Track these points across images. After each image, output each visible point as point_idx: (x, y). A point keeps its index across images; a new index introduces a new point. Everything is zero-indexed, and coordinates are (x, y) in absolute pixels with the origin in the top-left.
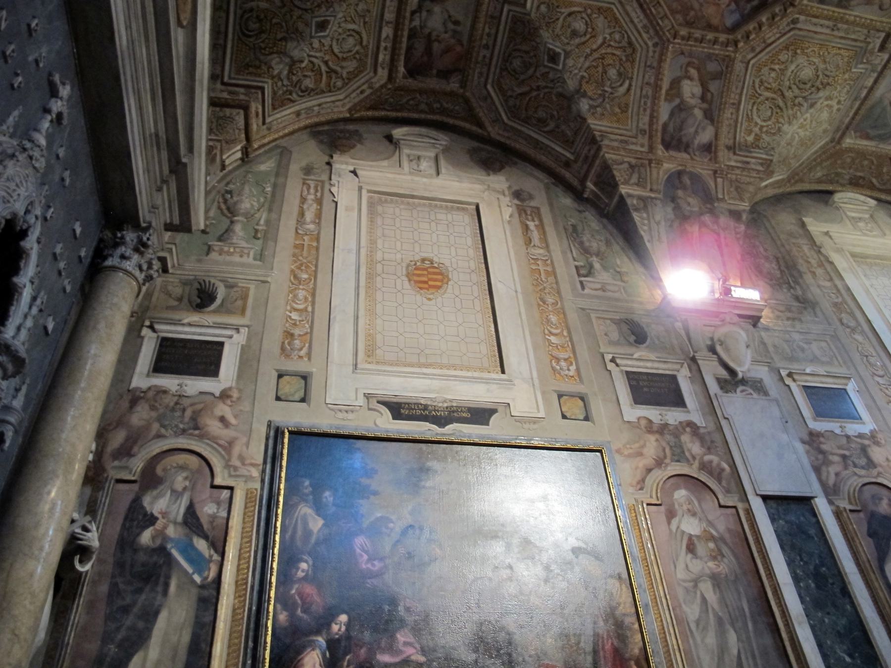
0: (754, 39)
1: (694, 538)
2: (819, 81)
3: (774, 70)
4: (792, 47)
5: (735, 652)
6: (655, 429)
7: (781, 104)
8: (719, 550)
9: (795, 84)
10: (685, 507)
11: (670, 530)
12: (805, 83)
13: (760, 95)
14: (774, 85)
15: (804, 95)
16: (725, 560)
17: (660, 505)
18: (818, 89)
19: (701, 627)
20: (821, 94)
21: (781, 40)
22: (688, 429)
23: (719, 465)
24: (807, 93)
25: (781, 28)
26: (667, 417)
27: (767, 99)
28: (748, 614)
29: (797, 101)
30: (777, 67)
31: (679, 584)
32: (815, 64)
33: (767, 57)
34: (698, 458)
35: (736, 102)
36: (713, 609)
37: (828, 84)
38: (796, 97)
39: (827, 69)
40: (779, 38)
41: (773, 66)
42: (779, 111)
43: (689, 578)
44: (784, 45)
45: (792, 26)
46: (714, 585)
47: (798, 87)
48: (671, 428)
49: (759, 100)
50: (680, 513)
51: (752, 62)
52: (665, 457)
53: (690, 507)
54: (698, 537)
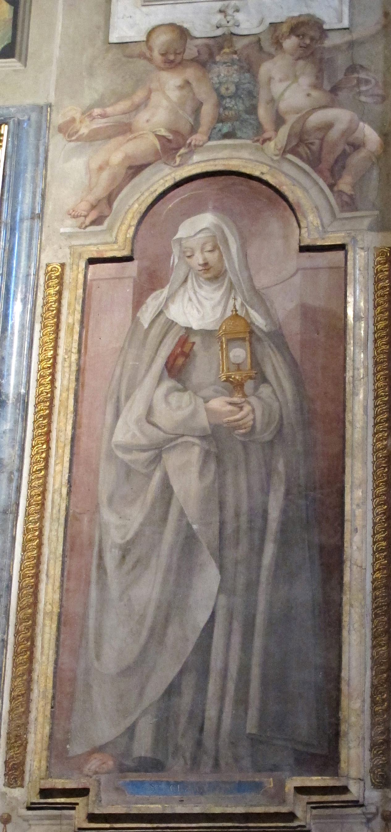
1: (196, 339)
5: (202, 618)
6: (191, 51)
8: (256, 363)
10: (198, 259)
11: (135, 320)
16: (265, 390)
17: (128, 259)
19: (130, 560)
22: (290, 43)
23: (350, 130)
26: (240, 16)
28: (273, 525)
31: (111, 456)
34: (291, 119)
36: (182, 513)
43: (144, 441)
46: (207, 454)
48: (239, 44)
50: (177, 275)
52: (194, 130)
53: (212, 258)
54: (207, 334)
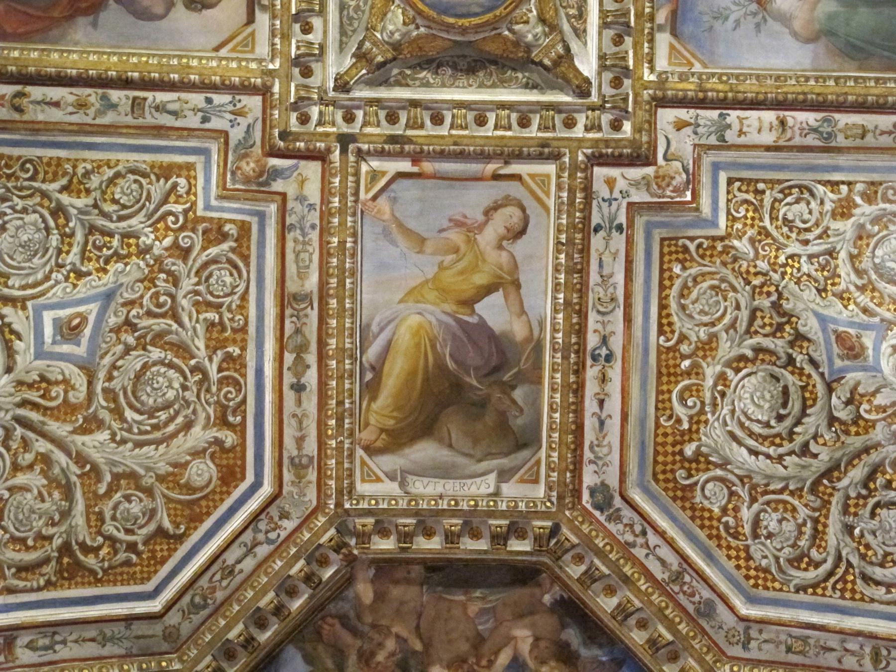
0: (671, 626)
2: (768, 343)
3: (756, 522)
4: (681, 474)
7: (857, 473)
9: (791, 433)
12: (785, 392)
13: (839, 558)
14: (803, 513)
15: (820, 389)
18: (799, 338)
20: (810, 326)
21: (663, 523)
24: (816, 377)
25: (629, 538)
27: (849, 529)
29: (843, 414)
30: (746, 514)
32: (722, 378)
33: (721, 555)
35: (868, 650)
37: (776, 306)
38: (832, 420)
39: (733, 325)
40: (662, 534)
41: (747, 529)
42: (880, 480)
44: (675, 508)
45: (618, 502)
47: (798, 422)
49: (855, 560)
51: (745, 610)
